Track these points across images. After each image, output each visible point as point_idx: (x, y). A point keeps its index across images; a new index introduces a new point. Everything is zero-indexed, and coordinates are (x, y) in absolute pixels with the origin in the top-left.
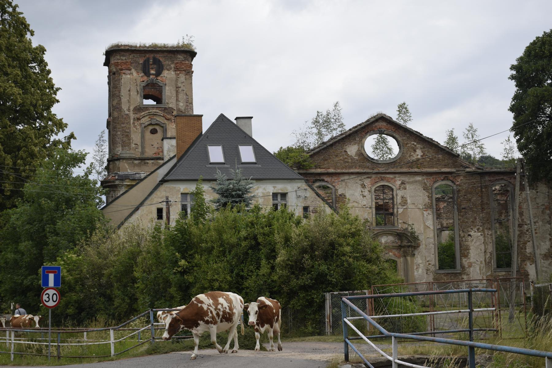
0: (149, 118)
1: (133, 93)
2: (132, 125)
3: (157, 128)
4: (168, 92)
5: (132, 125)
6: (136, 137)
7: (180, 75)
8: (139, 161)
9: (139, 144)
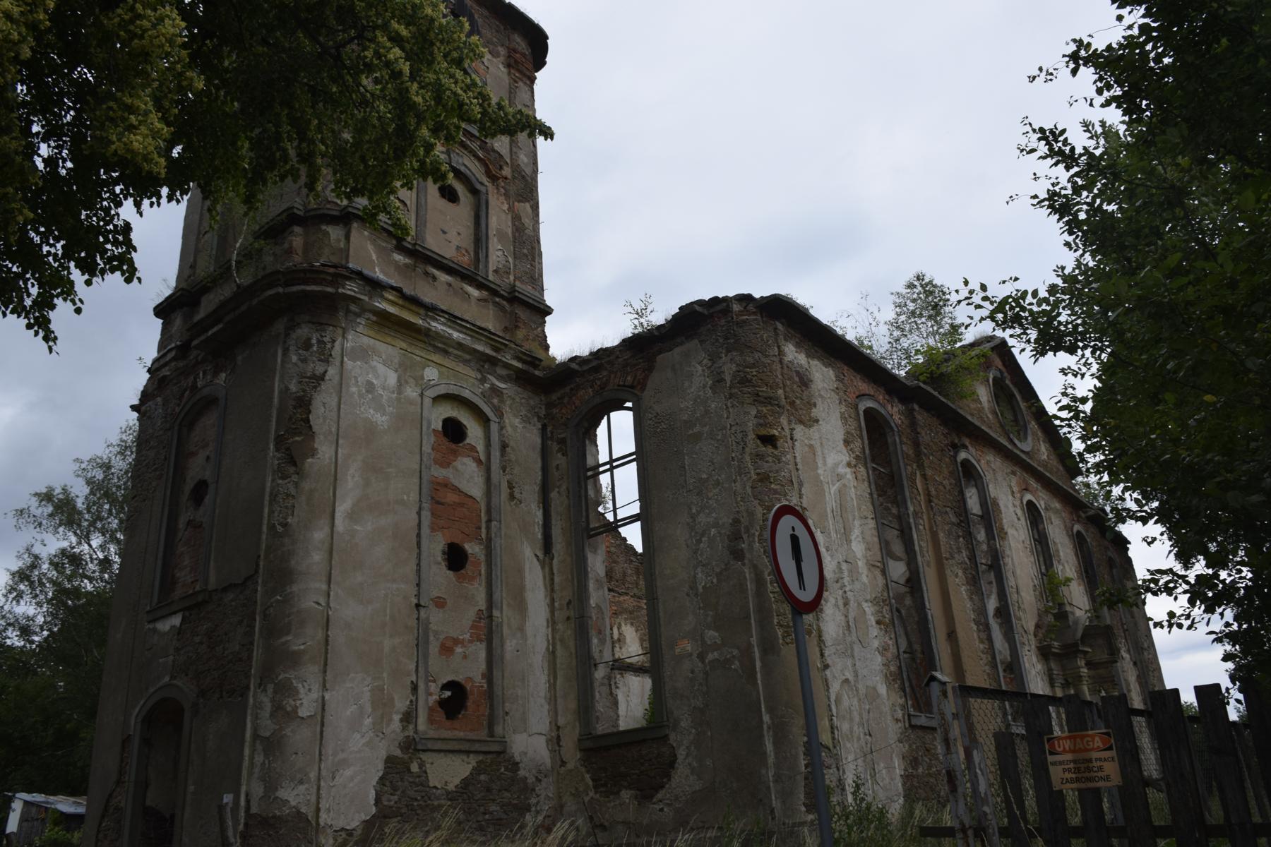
3: (459, 188)
7: (521, 84)
8: (407, 261)
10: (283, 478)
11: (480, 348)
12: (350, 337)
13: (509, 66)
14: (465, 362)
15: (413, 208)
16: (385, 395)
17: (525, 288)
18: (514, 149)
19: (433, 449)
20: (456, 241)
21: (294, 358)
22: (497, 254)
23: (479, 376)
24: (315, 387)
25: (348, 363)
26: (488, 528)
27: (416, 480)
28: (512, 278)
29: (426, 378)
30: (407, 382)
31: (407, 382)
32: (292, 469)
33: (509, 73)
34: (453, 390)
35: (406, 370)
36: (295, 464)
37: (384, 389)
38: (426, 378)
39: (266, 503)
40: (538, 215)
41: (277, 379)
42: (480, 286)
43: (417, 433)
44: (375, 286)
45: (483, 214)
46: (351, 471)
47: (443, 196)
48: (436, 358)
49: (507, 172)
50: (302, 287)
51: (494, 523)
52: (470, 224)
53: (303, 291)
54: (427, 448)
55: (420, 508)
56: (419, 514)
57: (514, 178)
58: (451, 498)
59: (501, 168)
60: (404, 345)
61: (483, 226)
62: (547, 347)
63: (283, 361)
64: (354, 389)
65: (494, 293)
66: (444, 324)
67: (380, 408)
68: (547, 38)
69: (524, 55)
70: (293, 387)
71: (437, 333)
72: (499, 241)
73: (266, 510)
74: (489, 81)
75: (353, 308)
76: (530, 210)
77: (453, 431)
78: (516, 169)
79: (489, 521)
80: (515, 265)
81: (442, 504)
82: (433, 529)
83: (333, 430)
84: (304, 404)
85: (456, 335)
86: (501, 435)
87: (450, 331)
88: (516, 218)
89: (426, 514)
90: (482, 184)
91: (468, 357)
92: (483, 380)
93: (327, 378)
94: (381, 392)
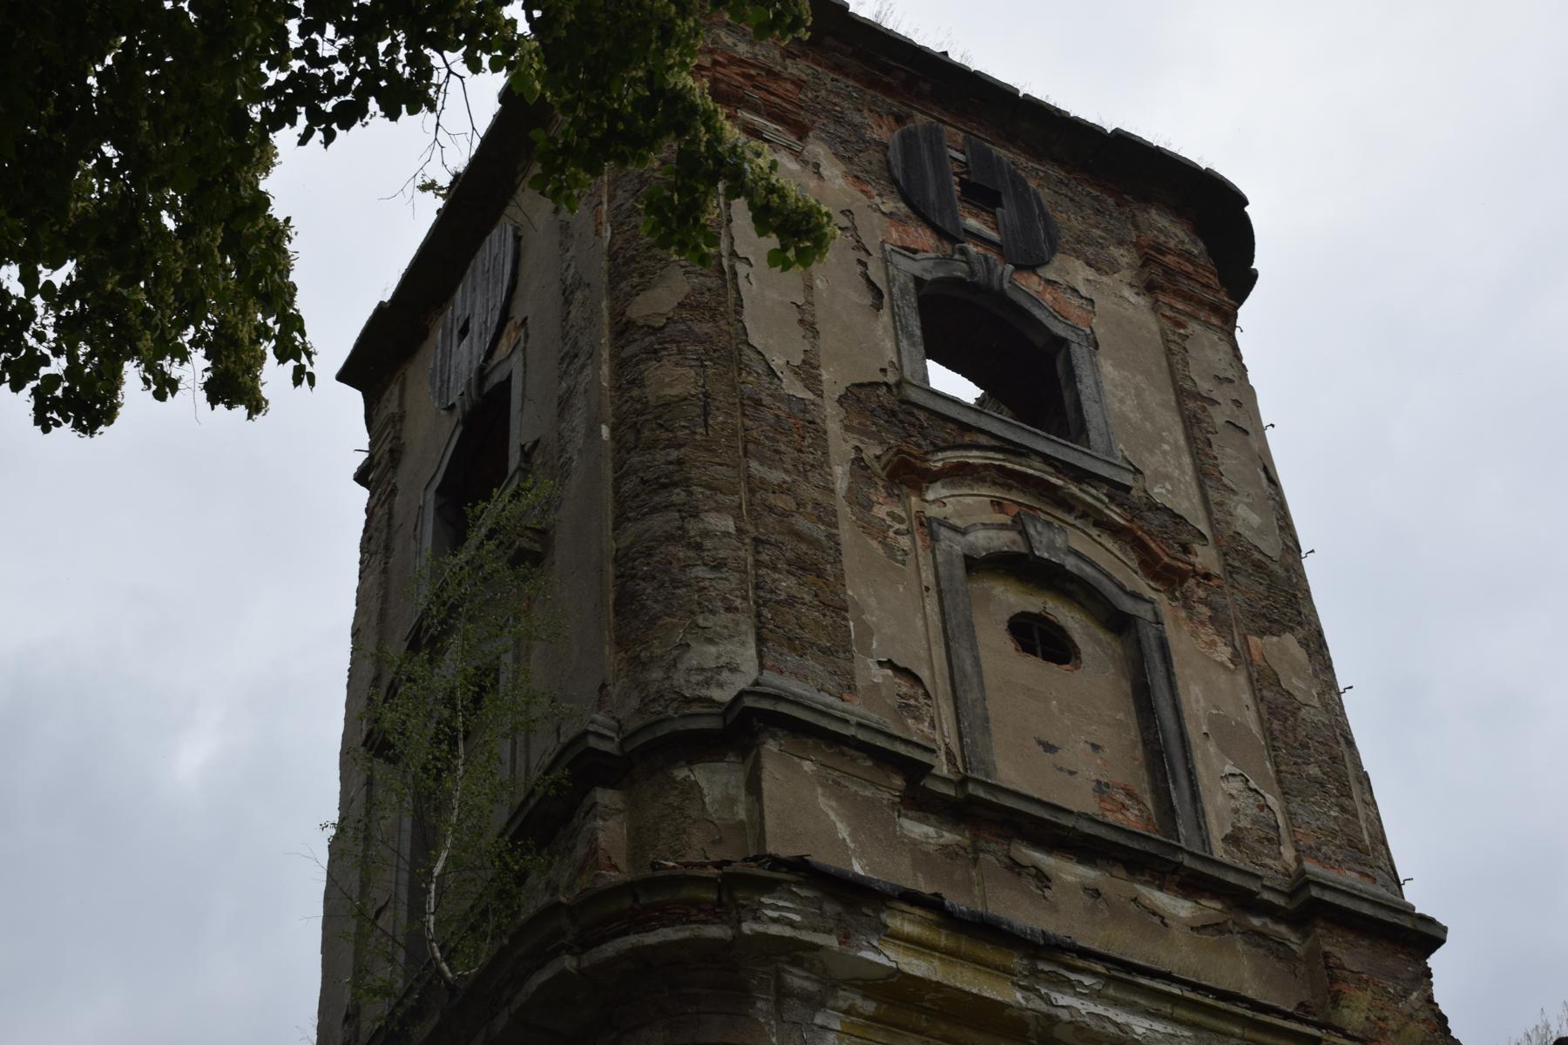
0: (998, 505)
2: (844, 509)
4: (1121, 392)
5: (844, 509)
6: (892, 613)
7: (1194, 327)
8: (949, 837)
9: (933, 672)
13: (1150, 288)
15: (943, 686)
18: (1214, 496)
20: (1090, 770)
28: (1288, 853)
33: (1155, 308)
40: (1328, 667)
42: (1193, 885)
44: (855, 898)
45: (1158, 679)
50: (633, 940)
52: (1125, 714)
53: (637, 952)
57: (1231, 571)
59: (1186, 549)
61: (1166, 713)
65: (1241, 900)
68: (1237, 200)
69: (1186, 256)
72: (1224, 750)
74: (1100, 332)
75: (797, 980)
76: (1300, 654)
78: (1234, 548)
80: (1290, 816)
87: (1122, 1017)
88: (1263, 680)
90: (1136, 596)
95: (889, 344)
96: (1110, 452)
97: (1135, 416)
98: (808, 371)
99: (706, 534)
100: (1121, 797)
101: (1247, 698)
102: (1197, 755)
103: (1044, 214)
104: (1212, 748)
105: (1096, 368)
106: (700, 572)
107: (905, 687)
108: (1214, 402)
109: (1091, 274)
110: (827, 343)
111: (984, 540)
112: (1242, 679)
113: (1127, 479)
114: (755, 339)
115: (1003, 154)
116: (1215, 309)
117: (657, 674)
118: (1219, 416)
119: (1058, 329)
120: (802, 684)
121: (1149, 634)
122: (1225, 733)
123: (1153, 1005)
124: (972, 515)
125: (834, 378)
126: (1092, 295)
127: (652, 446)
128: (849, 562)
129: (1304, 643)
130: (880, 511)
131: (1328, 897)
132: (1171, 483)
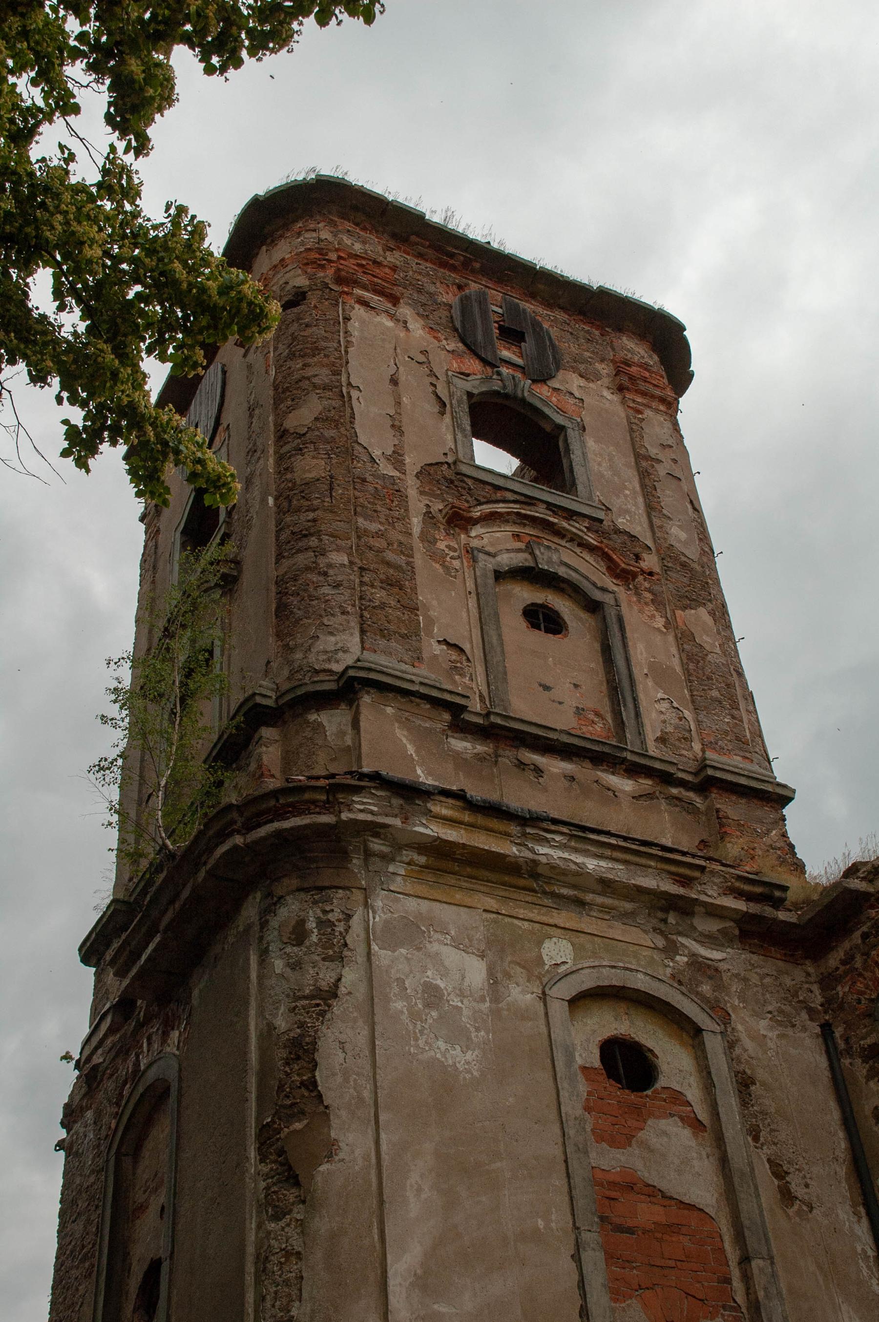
0: (517, 536)
1: (418, 404)
2: (418, 546)
5: (418, 546)
6: (447, 608)
7: (648, 413)
8: (480, 748)
9: (472, 646)
10: (276, 1218)
11: (649, 882)
12: (379, 904)
13: (621, 389)
14: (626, 917)
15: (478, 653)
16: (467, 1008)
17: (730, 762)
18: (657, 522)
19: (587, 1109)
20: (572, 700)
21: (279, 965)
22: (658, 711)
23: (661, 942)
24: (322, 1014)
25: (382, 955)
26: (747, 1278)
27: (559, 1181)
28: (697, 746)
29: (548, 962)
30: (508, 976)
31: (508, 976)
32: (291, 1195)
33: (623, 401)
34: (614, 978)
35: (504, 953)
36: (297, 1184)
37: (462, 995)
38: (548, 962)
39: (250, 1279)
40: (729, 626)
41: (252, 1012)
42: (634, 770)
43: (545, 1076)
44: (410, 793)
46: (414, 1178)
47: (535, 626)
48: (563, 918)
49: (650, 562)
50: (276, 825)
51: (756, 1264)
52: (596, 664)
53: (279, 833)
54: (573, 1108)
55: (578, 1245)
56: (577, 1258)
57: (666, 569)
58: (647, 1213)
59: (638, 557)
60: (491, 903)
62: (799, 867)
63: (260, 977)
64: (399, 1005)
65: (666, 778)
66: (563, 847)
67: (458, 1035)
68: (680, 328)
69: (645, 367)
70: (282, 1023)
71: (553, 867)
72: (658, 684)
73: (250, 1297)
74: (587, 420)
75: (377, 845)
76: (709, 620)
77: (627, 1065)
78: (670, 556)
79: (745, 1260)
80: (699, 722)
81: (630, 1231)
82: (616, 1295)
83: (367, 1094)
84: (303, 1050)
85: (591, 864)
86: (732, 1060)
87: (579, 859)
88: (684, 637)
89: (593, 1258)
90: (603, 590)
91: (628, 906)
92: (671, 949)
93: (342, 990)
94: (456, 1002)
95: (449, 437)
96: (590, 498)
97: (608, 474)
98: (396, 458)
99: (330, 566)
100: (591, 716)
101: (674, 650)
102: (640, 688)
103: (553, 345)
104: (650, 683)
105: (583, 444)
106: (326, 590)
107: (454, 655)
108: (659, 461)
109: (582, 382)
110: (410, 437)
111: (506, 560)
112: (671, 638)
113: (601, 515)
114: (362, 439)
115: (529, 307)
116: (663, 400)
117: (299, 655)
118: (661, 471)
119: (559, 420)
120: (388, 660)
121: (611, 613)
122: (659, 673)
123: (599, 851)
124: (499, 544)
125: (413, 461)
126: (583, 397)
127: (298, 510)
128: (421, 578)
129: (712, 613)
130: (441, 545)
131: (718, 774)
132: (630, 517)
